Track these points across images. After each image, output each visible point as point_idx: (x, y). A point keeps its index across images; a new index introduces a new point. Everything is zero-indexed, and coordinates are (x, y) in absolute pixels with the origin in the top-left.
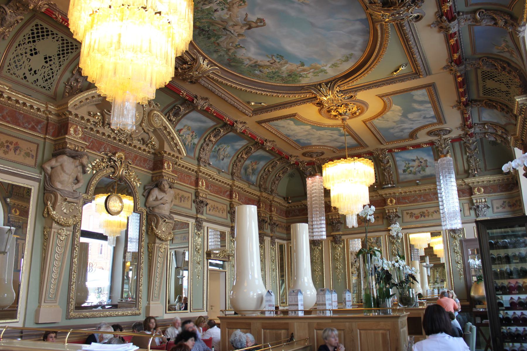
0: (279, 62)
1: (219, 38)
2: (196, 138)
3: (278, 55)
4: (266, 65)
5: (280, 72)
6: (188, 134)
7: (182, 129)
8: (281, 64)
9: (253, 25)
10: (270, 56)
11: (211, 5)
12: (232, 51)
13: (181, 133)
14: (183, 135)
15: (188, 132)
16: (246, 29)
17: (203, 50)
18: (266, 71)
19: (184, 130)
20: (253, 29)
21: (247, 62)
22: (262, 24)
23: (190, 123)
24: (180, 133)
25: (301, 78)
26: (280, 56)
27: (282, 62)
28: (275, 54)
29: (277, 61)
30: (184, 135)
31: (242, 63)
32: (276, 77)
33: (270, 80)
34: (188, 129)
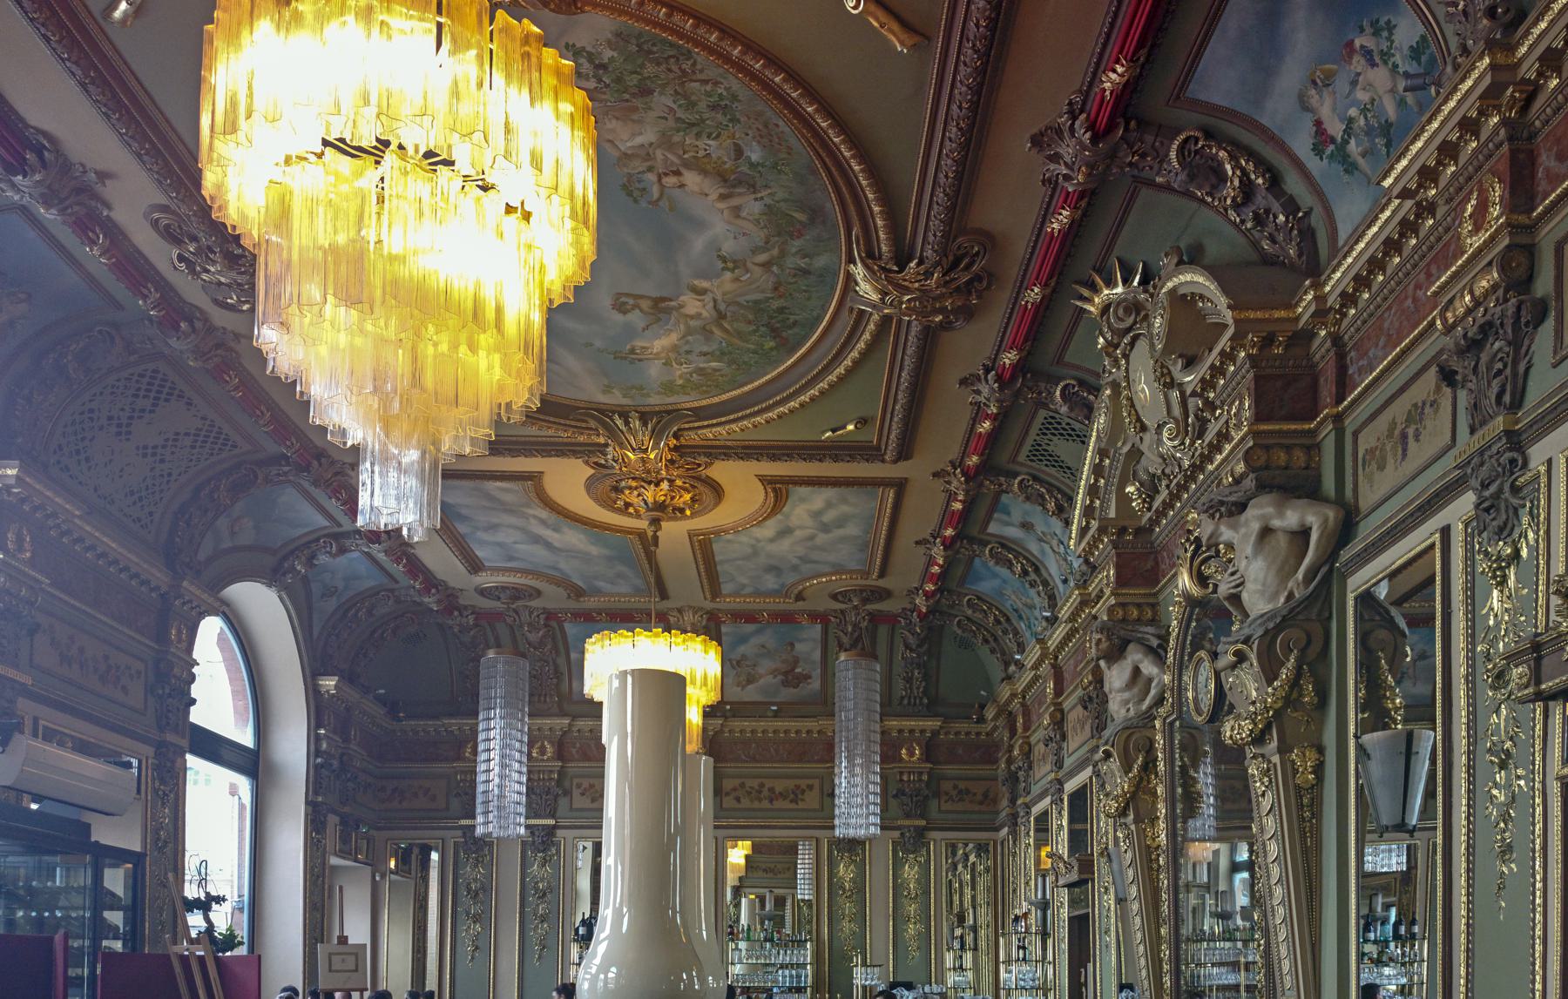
0: (650, 169)
1: (756, 302)
2: (1390, 28)
3: (636, 201)
4: (704, 172)
5: (671, 123)
6: (1354, 83)
7: (1318, 123)
8: (648, 157)
9: (645, 304)
10: (664, 204)
11: (701, 365)
12: (762, 258)
13: (1336, 129)
14: (1351, 121)
15: (1341, 84)
16: (671, 300)
17: (833, 289)
18: (715, 148)
19: (1325, 112)
20: (655, 294)
21: (752, 207)
22: (623, 299)
23: (1291, 76)
24: (1333, 140)
25: (608, 54)
26: (630, 194)
27: (638, 166)
28: (644, 204)
29: (652, 177)
30: (1353, 112)
31: (770, 210)
32: (702, 105)
33: (734, 98)
34: (1328, 80)
